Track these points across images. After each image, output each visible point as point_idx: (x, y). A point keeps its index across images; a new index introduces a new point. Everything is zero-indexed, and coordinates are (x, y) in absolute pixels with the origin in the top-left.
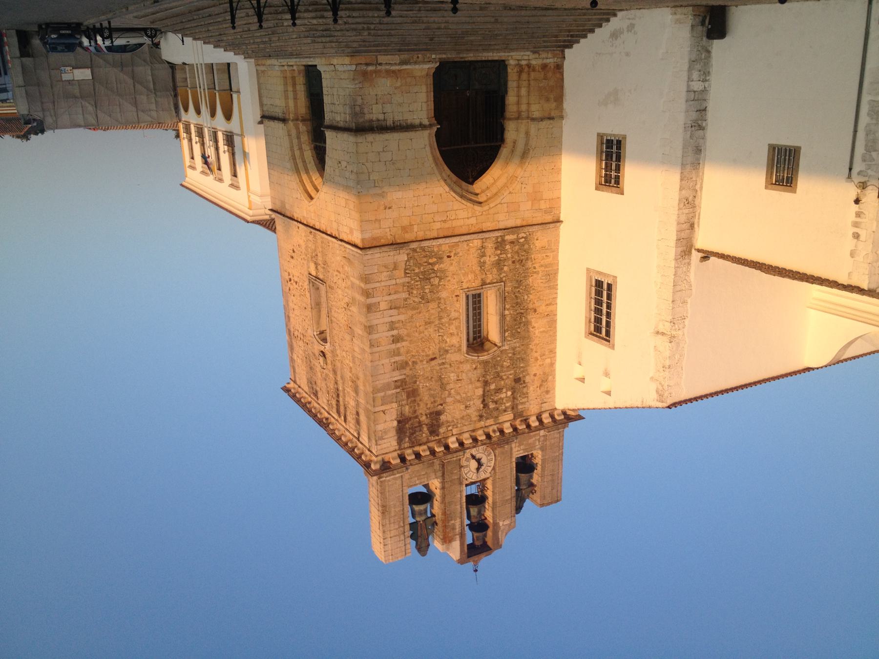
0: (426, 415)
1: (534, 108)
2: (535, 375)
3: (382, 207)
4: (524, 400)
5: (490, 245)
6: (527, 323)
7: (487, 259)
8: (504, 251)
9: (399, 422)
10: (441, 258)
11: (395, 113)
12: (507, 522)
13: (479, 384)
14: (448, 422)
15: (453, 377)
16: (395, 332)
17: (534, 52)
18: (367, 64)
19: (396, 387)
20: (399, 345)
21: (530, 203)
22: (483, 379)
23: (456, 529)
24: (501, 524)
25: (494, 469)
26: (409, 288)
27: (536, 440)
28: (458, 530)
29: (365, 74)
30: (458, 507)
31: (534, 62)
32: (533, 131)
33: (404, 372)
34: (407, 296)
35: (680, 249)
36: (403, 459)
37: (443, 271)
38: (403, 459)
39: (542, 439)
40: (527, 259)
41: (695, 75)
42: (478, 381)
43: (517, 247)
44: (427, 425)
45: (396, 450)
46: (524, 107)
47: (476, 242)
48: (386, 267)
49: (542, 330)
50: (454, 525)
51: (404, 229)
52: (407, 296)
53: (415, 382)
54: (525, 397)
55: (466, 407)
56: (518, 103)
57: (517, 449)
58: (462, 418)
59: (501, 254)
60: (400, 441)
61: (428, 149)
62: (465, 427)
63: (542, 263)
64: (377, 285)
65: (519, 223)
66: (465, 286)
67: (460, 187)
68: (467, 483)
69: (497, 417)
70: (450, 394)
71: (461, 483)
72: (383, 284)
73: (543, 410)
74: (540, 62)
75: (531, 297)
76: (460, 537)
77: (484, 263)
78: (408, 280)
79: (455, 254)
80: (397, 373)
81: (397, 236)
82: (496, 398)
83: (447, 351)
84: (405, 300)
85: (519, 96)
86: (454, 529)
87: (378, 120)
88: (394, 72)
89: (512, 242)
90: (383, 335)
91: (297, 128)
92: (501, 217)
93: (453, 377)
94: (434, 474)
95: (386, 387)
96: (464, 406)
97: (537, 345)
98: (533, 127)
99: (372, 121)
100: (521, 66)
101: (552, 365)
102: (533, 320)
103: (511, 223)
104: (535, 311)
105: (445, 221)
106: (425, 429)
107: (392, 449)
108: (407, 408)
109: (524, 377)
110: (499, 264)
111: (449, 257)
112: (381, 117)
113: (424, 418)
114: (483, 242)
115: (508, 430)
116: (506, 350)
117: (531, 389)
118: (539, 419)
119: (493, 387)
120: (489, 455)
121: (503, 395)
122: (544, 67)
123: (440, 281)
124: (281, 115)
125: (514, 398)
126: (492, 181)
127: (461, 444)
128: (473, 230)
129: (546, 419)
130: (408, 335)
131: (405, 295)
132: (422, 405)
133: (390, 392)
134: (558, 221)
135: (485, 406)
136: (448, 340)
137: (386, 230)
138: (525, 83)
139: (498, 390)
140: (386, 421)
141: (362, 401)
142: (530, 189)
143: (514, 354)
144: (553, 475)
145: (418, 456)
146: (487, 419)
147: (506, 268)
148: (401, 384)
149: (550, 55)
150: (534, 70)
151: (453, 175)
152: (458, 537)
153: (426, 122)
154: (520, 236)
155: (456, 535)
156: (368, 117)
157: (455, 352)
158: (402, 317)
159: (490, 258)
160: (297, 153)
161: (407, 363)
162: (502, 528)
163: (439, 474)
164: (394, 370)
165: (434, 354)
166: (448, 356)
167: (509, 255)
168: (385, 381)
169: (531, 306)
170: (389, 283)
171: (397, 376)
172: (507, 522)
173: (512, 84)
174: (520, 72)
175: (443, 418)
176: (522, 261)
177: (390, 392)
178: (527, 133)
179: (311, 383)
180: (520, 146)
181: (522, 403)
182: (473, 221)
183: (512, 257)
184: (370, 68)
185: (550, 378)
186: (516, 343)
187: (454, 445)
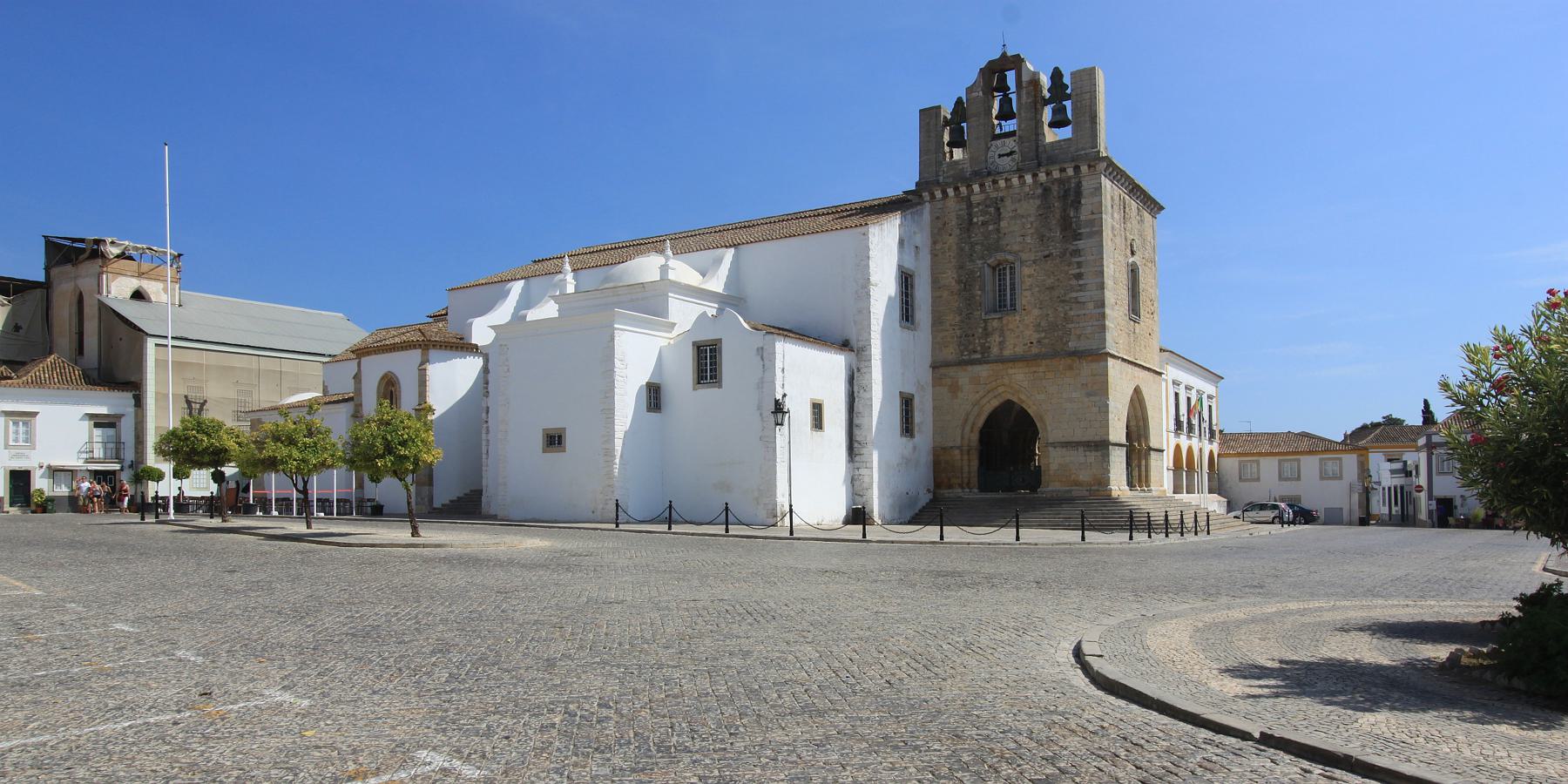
0: (1054, 206)
1: (959, 457)
2: (950, 235)
3: (1089, 385)
4: (960, 213)
5: (995, 350)
6: (959, 282)
7: (998, 339)
8: (982, 345)
9: (1080, 202)
10: (1039, 342)
11: (1077, 457)
12: (975, 94)
13: (1003, 231)
14: (1034, 198)
15: (1028, 240)
16: (1081, 282)
17: (960, 497)
18: (1098, 490)
19: (1079, 234)
20: (1078, 271)
21: (960, 383)
22: (1000, 235)
23: (1026, 93)
24: (981, 93)
25: (989, 149)
26: (1067, 319)
29: (1100, 484)
30: (1023, 115)
31: (960, 490)
32: (959, 439)
33: (1073, 247)
34: (1069, 312)
35: (867, 353)
36: (1077, 169)
37: (1038, 331)
38: (1077, 169)
39: (941, 173)
40: (961, 337)
41: (866, 479)
42: (1005, 234)
43: (971, 347)
45: (1084, 176)
46: (966, 457)
47: (1007, 353)
48: (1088, 338)
49: (944, 275)
50: (1028, 98)
51: (1071, 368)
52: (1069, 312)
53: (1063, 237)
54: (959, 215)
55: (1016, 210)
56: (969, 460)
57: (966, 166)
58: (1020, 200)
59: (984, 343)
60: (1079, 185)
61: (1049, 428)
62: (1017, 192)
63: (946, 333)
64: (1095, 323)
65: (970, 368)
66: (1017, 318)
67: (1020, 399)
68: (1014, 138)
69: (985, 199)
70: (1032, 224)
71: (1019, 136)
72: (1090, 324)
73: (942, 202)
74: (955, 491)
75: (956, 304)
76: (1022, 85)
77: (1000, 336)
78: (1070, 326)
79: (1027, 344)
80: (1081, 247)
81: (1078, 362)
82: (987, 217)
83: (1034, 262)
84: (1071, 309)
85: (969, 466)
86: (1028, 93)
87: (1090, 451)
88: (1077, 486)
89: (975, 352)
90: (1089, 280)
92: (984, 374)
93: (1028, 240)
94: (1047, 149)
95: (1090, 235)
96: (1018, 211)
97: (950, 262)
98: (958, 443)
99: (1097, 451)
100: (969, 488)
101: (934, 243)
102: (954, 283)
103: (977, 368)
104: (952, 292)
105: (1035, 372)
107: (1086, 178)
108: (1072, 214)
109: (961, 234)
110: (986, 334)
111: (1032, 343)
112: (1088, 453)
113: (1056, 205)
114: (1001, 353)
115: (976, 188)
116: (979, 260)
117: (953, 223)
118: (945, 193)
119: (991, 228)
121: (981, 218)
122: (950, 487)
123: (1040, 323)
124: (1152, 452)
125: (970, 215)
126: (991, 402)
127: (1021, 177)
128: (1010, 364)
129: (938, 194)
130: (1070, 279)
131: (1072, 313)
132: (1058, 216)
133: (1088, 230)
134: (935, 367)
135: (998, 209)
136: (1033, 272)
137: (1086, 369)
138: (964, 475)
139: (983, 223)
140: (1092, 204)
141: (1110, 220)
142: (960, 394)
143: (971, 255)
144: (929, 137)
146: (996, 198)
147: (980, 330)
148: (1077, 236)
149: (947, 495)
150: (959, 484)
151: (1026, 408)
153: (1051, 449)
154: (967, 357)
156: (1099, 454)
157: (1026, 261)
158: (1074, 295)
159: (996, 338)
160: (1141, 423)
161: (1071, 255)
164: (1083, 249)
165: (1046, 261)
166: (1033, 258)
167: (977, 341)
168: (1090, 240)
169: (956, 297)
170: (1085, 324)
171: (1081, 244)
172: (975, 94)
173: (974, 474)
174: (968, 484)
175: (1038, 202)
176: (965, 336)
177: (1088, 230)
178: (962, 438)
179: (1141, 221)
180: (968, 428)
181: (960, 210)
182: (1011, 371)
183: (975, 339)
185: (936, 231)
186: (969, 266)
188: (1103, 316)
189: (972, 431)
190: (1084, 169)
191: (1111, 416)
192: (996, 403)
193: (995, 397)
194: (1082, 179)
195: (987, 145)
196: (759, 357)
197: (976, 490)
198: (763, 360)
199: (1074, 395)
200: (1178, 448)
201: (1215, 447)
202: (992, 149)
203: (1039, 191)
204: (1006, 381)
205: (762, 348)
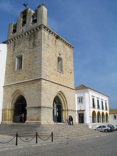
65: (11, 86)
91: (65, 108)
105: (25, 86)
118: (10, 41)
129: (9, 42)
156: (38, 110)
160: (65, 103)
184: (37, 121)
187: (26, 34)
188: (41, 67)
189: (12, 104)
190: (38, 28)
191: (42, 98)
192: (17, 96)
193: (17, 94)
197: (12, 122)
199: (33, 92)
200: (94, 113)
201: (108, 112)
203: (29, 37)
204: (18, 89)
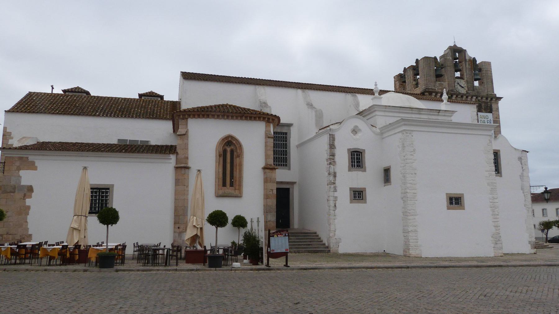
24: (451, 58)
27: (439, 87)
28: (467, 63)
30: (467, 72)
38: (492, 99)
44: (483, 108)
45: (493, 103)
57: (446, 86)
60: (491, 106)
86: (469, 64)
106: (483, 107)
120: (457, 88)
127: (472, 97)
140: (496, 114)
145: (487, 99)
152: (467, 60)
155: (468, 61)
162: (450, 56)
163: (475, 88)
190: (494, 99)
194: (492, 104)
195: (454, 80)
196: (520, 162)
198: (522, 164)
202: (456, 82)
205: (521, 158)
